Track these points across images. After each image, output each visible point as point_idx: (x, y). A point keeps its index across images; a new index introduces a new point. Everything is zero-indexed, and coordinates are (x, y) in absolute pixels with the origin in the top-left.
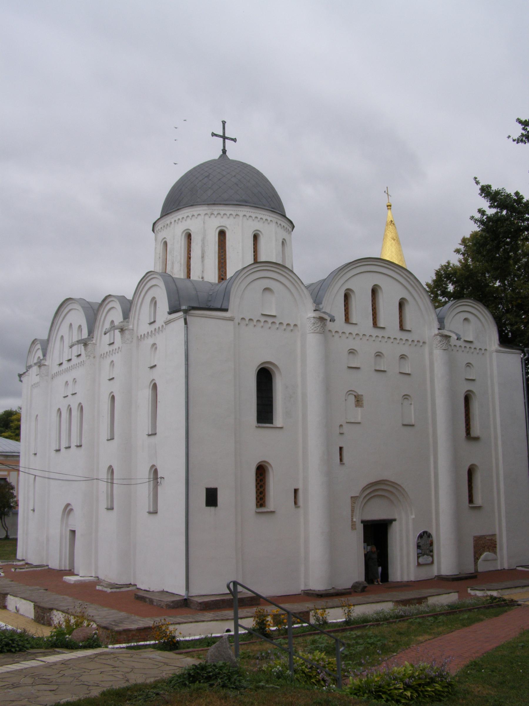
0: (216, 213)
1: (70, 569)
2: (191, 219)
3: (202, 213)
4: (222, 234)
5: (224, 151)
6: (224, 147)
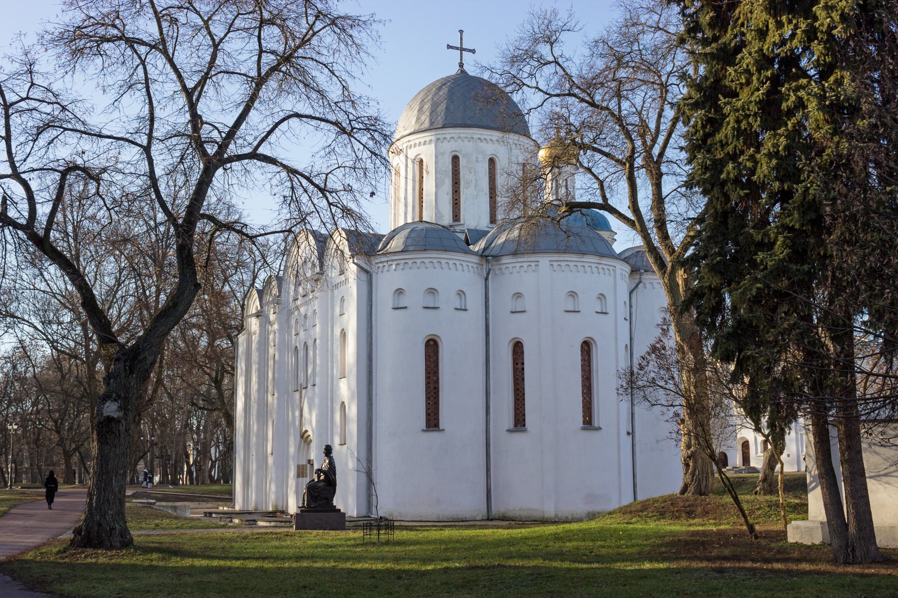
5: (461, 65)
6: (461, 59)
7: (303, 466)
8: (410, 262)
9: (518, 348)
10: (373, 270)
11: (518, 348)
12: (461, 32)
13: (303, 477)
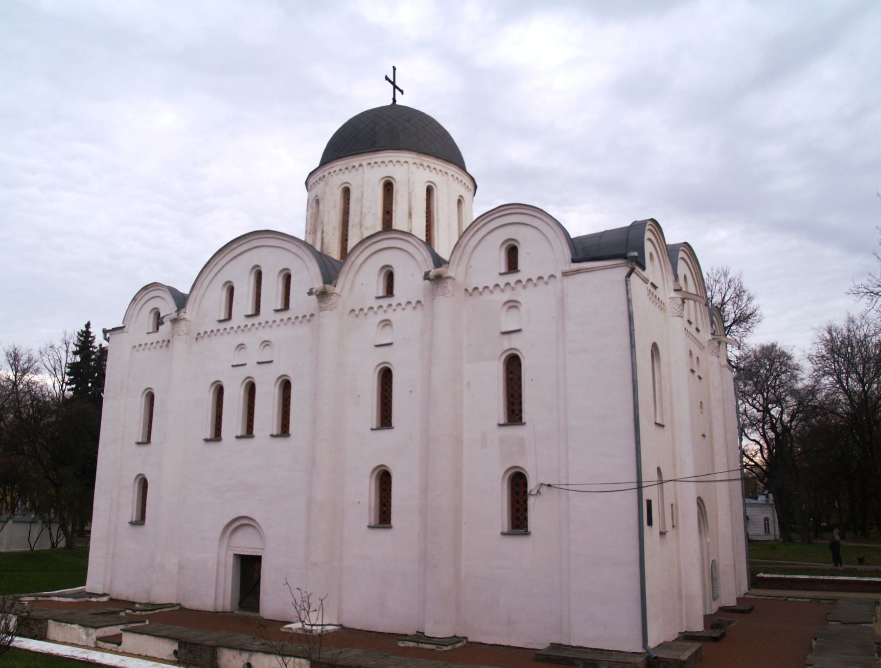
1: (232, 611)
3: (411, 161)
4: (429, 191)
5: (394, 100)
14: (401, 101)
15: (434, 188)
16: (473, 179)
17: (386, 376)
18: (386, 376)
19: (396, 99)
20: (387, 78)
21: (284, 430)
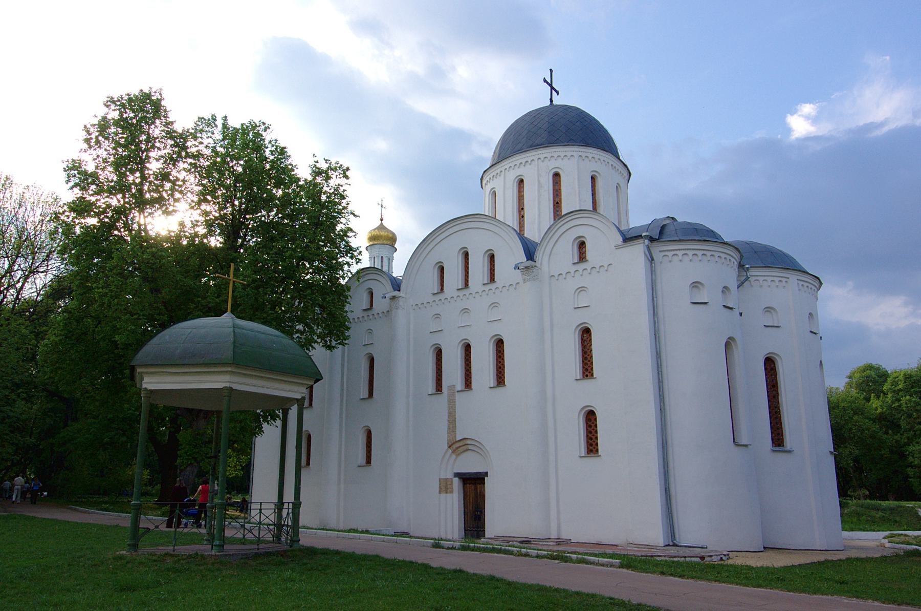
0: (590, 156)
2: (524, 166)
5: (551, 101)
7: (446, 480)
8: (709, 254)
9: (770, 364)
10: (657, 256)
11: (770, 364)
12: (551, 71)
13: (447, 493)
14: (557, 101)
15: (599, 177)
16: (625, 166)
17: (586, 333)
18: (586, 333)
19: (553, 99)
20: (545, 81)
21: (500, 379)
